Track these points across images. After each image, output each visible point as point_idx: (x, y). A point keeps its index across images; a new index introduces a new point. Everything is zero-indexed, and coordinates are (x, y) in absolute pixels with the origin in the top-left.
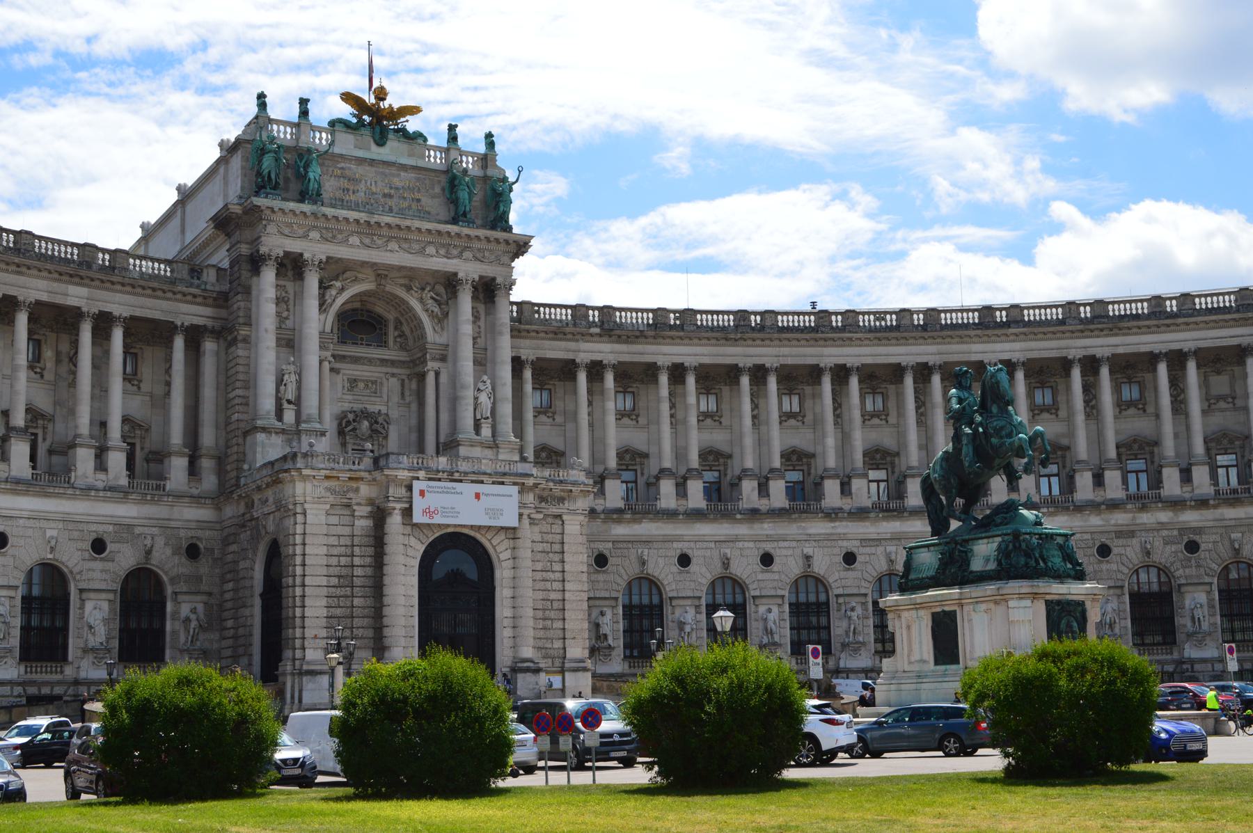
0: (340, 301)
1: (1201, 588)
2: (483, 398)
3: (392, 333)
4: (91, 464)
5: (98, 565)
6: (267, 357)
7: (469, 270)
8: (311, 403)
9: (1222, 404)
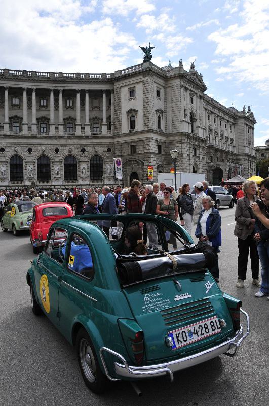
1: (85, 163)
9: (96, 109)
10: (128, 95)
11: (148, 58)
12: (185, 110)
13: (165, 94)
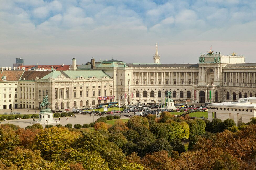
0: (207, 70)
7: (215, 66)
8: (203, 79)
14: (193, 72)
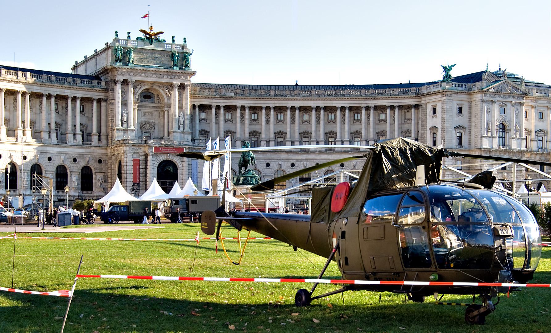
0: (140, 91)
2: (181, 119)
3: (156, 98)
4: (72, 138)
5: (75, 165)
6: (119, 108)
10: (432, 112)
11: (447, 77)
12: (488, 124)
13: (470, 108)
14: (77, 96)
